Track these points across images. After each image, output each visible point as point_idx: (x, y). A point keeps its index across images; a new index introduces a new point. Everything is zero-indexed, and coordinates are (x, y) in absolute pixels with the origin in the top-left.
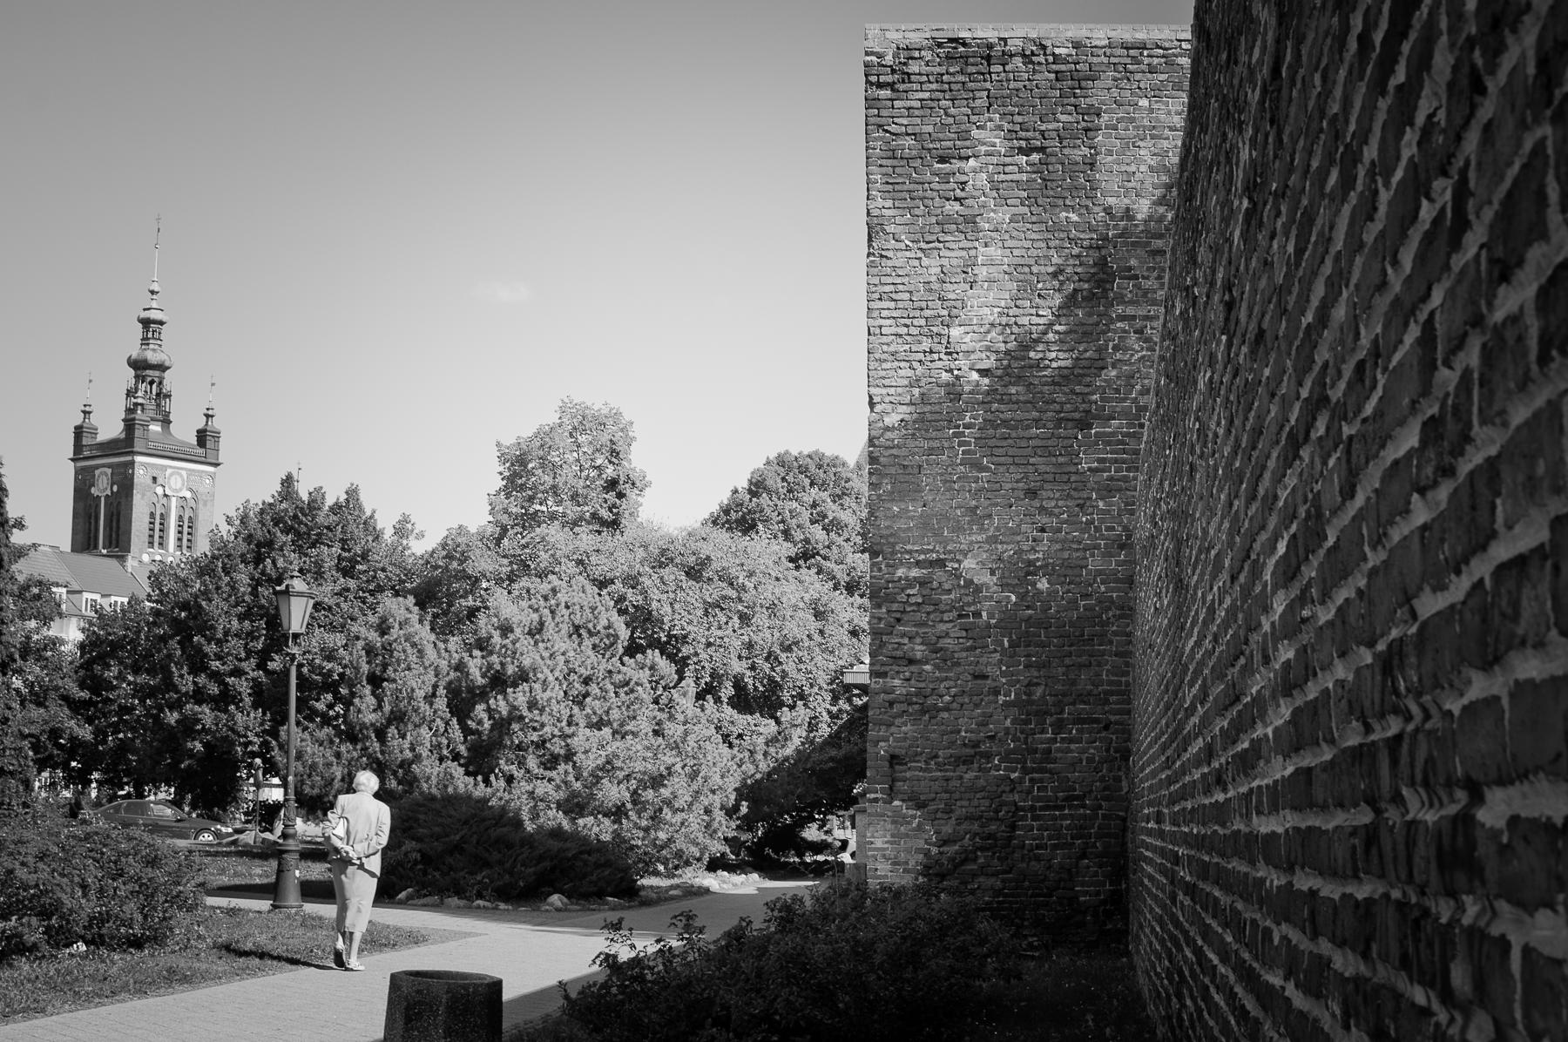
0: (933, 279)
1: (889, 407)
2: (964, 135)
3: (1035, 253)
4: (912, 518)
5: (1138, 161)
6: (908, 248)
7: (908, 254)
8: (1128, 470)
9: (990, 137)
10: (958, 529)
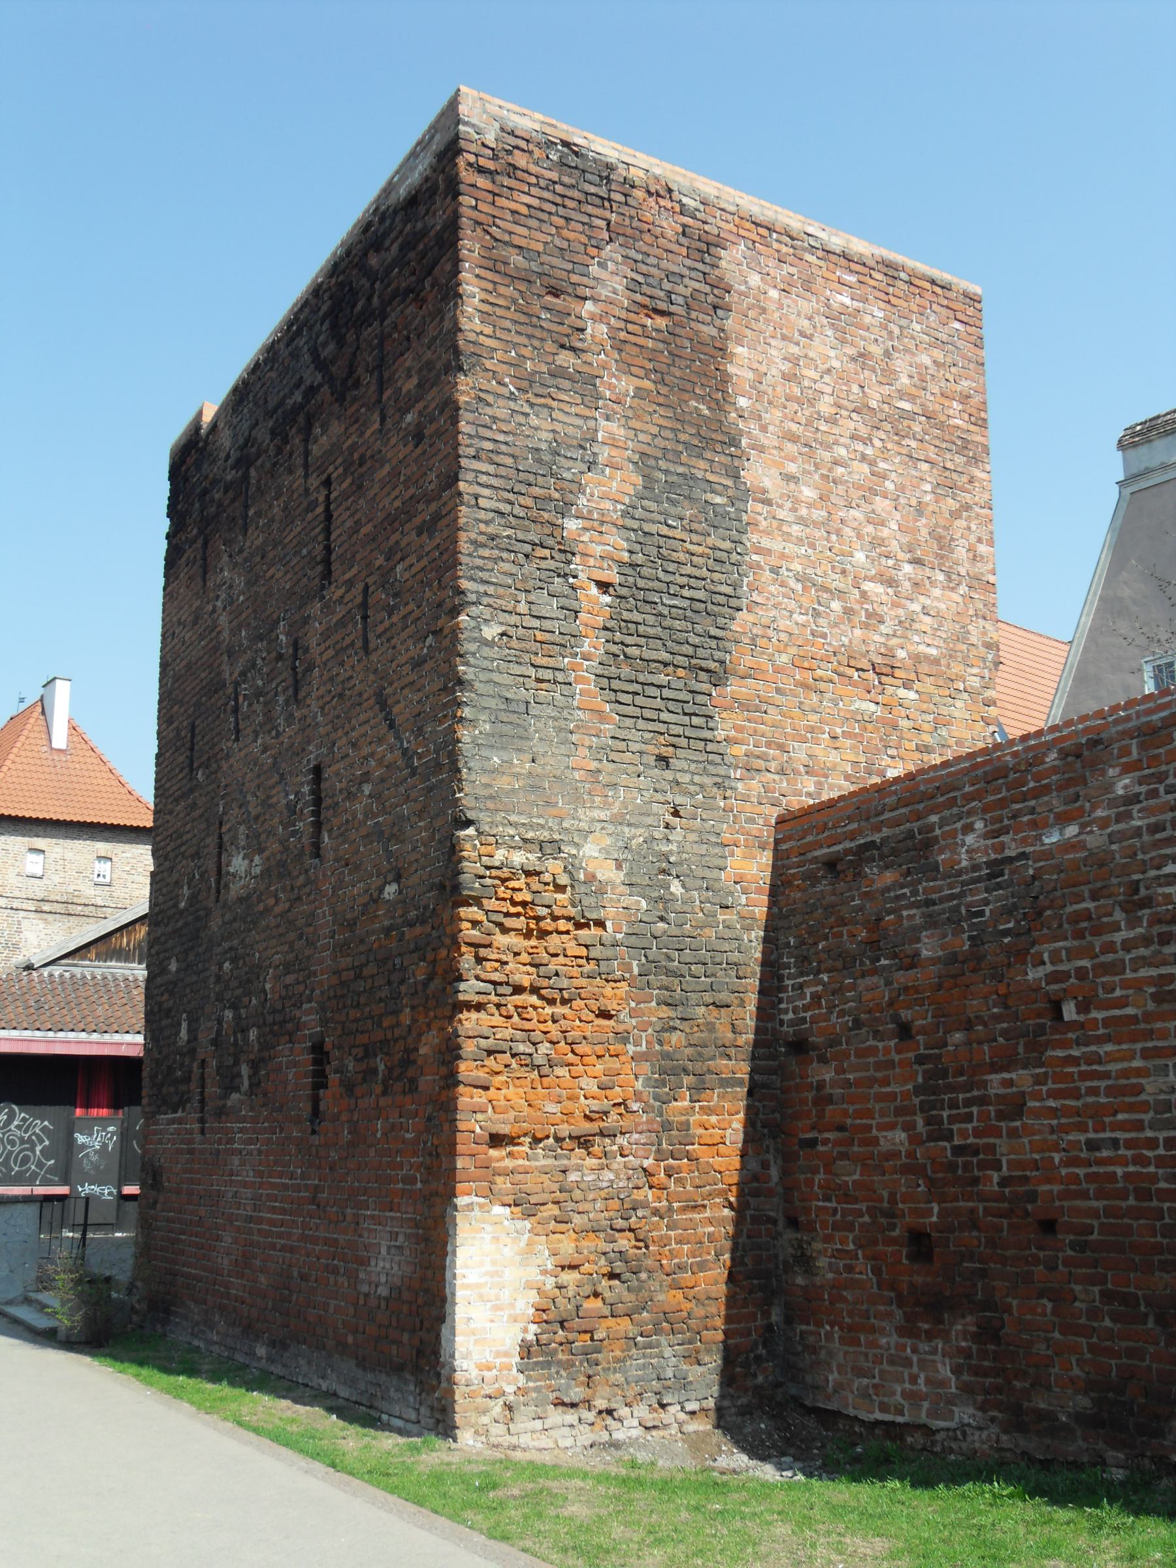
0: (544, 446)
1: (487, 613)
3: (663, 443)
4: (517, 776)
5: (770, 362)
6: (512, 397)
7: (512, 404)
8: (769, 745)
10: (576, 799)
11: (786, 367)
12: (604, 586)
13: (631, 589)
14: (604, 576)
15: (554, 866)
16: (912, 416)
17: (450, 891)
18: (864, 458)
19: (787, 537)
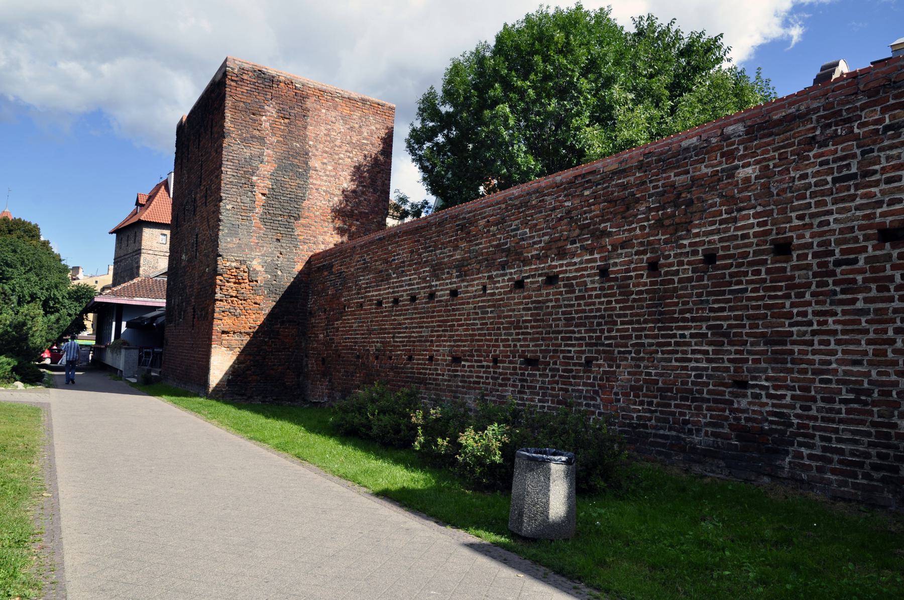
2: (262, 107)
5: (321, 131)
9: (271, 110)
10: (252, 250)
11: (326, 132)
12: (263, 194)
13: (271, 196)
14: (264, 192)
15: (244, 267)
16: (367, 144)
17: (215, 272)
18: (349, 157)
19: (321, 180)
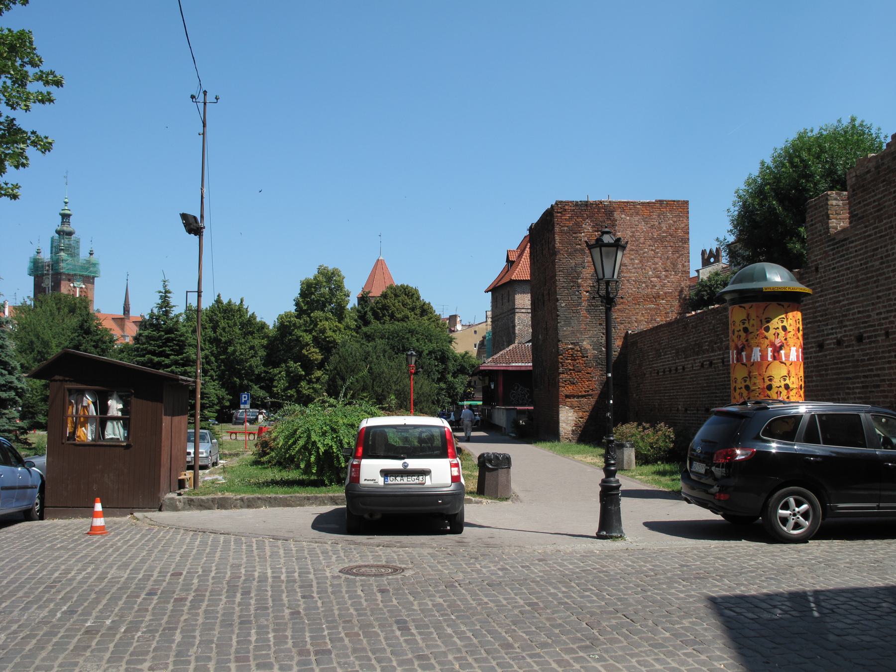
12: (587, 292)
15: (578, 348)
16: (666, 237)
17: (558, 353)
